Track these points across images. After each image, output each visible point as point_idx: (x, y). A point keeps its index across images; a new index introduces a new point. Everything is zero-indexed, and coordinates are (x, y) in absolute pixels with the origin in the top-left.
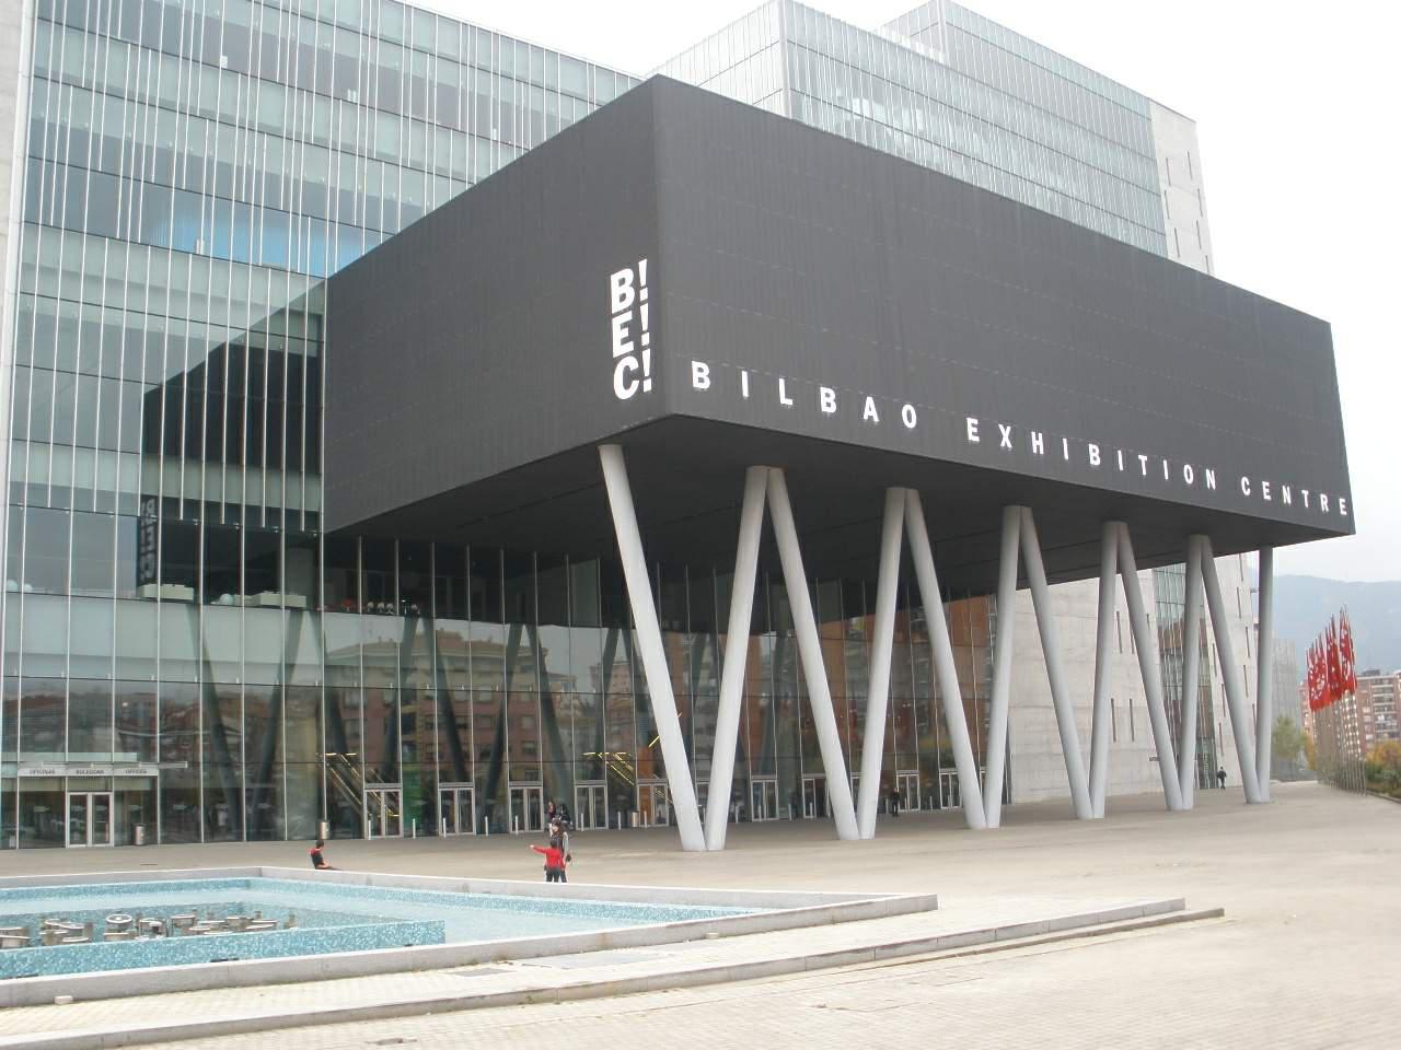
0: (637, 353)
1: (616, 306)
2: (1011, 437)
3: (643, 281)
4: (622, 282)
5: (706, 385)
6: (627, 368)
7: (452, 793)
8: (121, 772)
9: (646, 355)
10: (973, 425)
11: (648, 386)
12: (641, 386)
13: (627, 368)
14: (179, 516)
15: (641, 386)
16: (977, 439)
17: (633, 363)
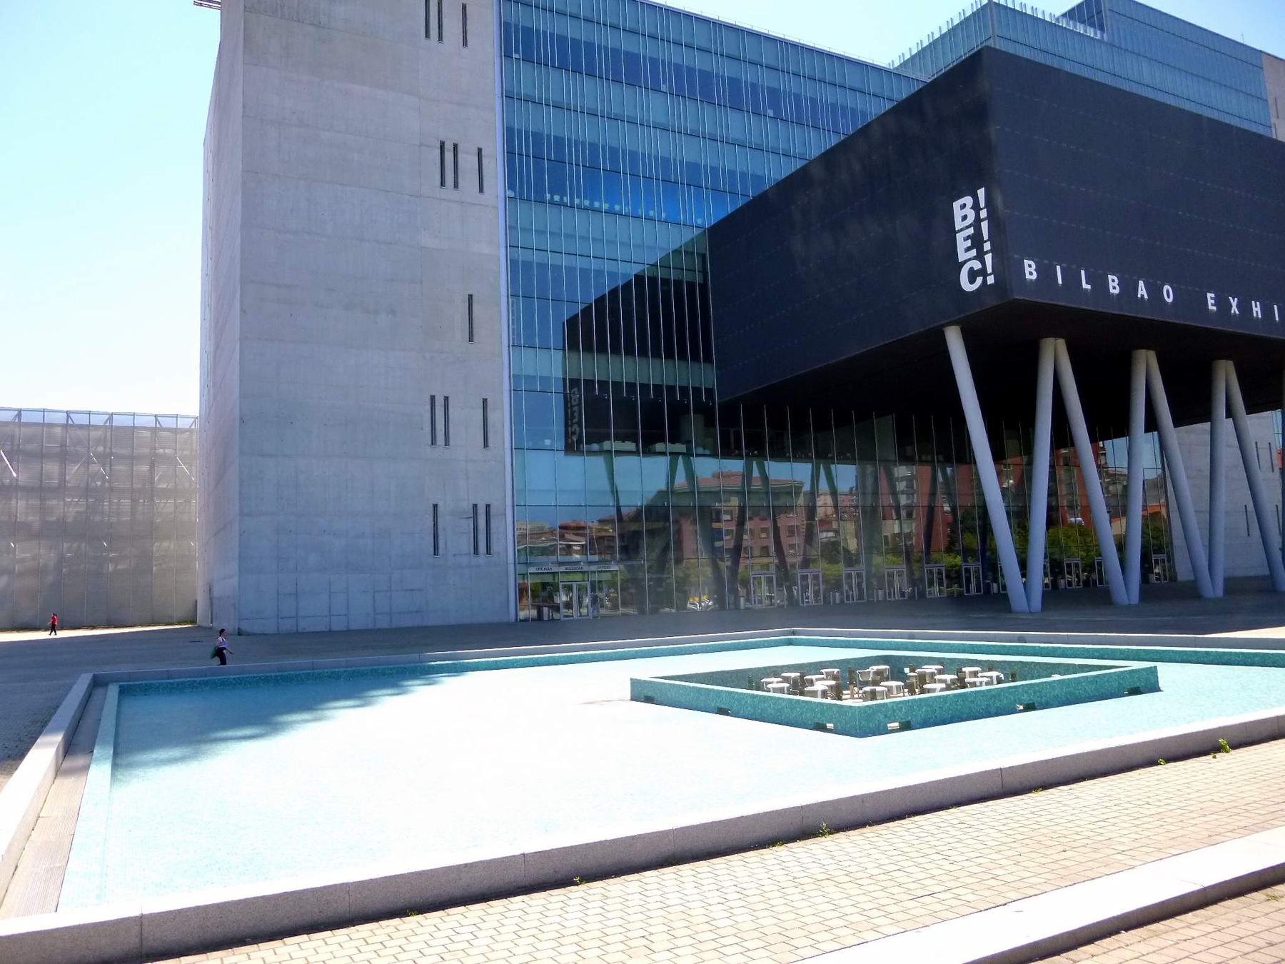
0: (980, 257)
1: (959, 224)
2: (1238, 306)
3: (982, 204)
4: (963, 206)
5: (1034, 277)
6: (971, 270)
7: (1071, 564)
8: (594, 568)
9: (988, 258)
10: (1211, 298)
11: (991, 280)
12: (985, 281)
13: (971, 270)
14: (622, 393)
15: (985, 281)
16: (1215, 308)
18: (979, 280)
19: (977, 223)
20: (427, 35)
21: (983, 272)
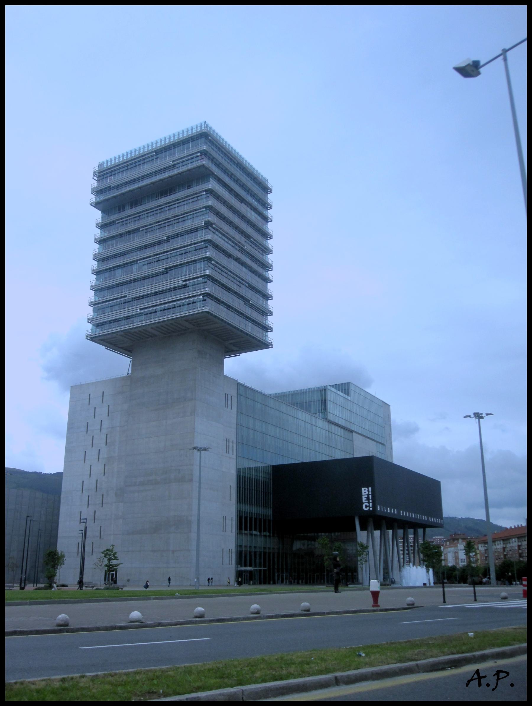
0: (369, 503)
1: (363, 494)
4: (365, 490)
9: (371, 504)
11: (371, 509)
12: (369, 509)
17: (368, 505)
18: (368, 508)
19: (368, 495)
20: (225, 407)
21: (369, 506)
